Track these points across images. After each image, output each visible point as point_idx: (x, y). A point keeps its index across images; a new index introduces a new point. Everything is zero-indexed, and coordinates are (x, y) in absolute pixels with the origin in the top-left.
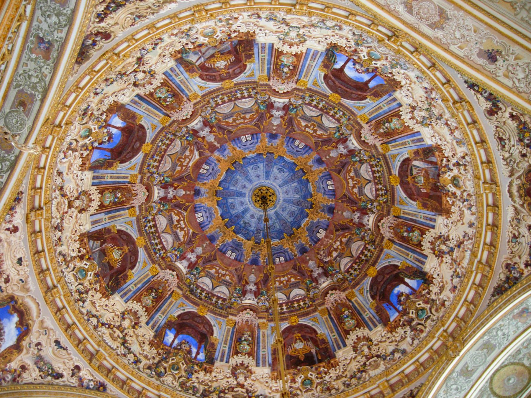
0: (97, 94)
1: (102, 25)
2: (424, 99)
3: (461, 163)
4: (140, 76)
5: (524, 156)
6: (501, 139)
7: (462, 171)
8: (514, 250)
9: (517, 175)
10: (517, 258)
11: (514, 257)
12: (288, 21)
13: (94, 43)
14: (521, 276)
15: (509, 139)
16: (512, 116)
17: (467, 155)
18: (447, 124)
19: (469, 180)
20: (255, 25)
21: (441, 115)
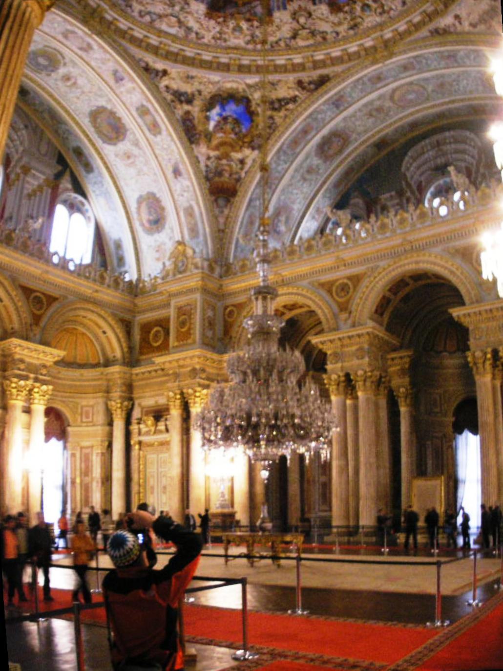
0: (337, 34)
1: (297, 93)
4: (302, 20)
12: (177, 24)
13: (310, 83)
20: (202, 25)
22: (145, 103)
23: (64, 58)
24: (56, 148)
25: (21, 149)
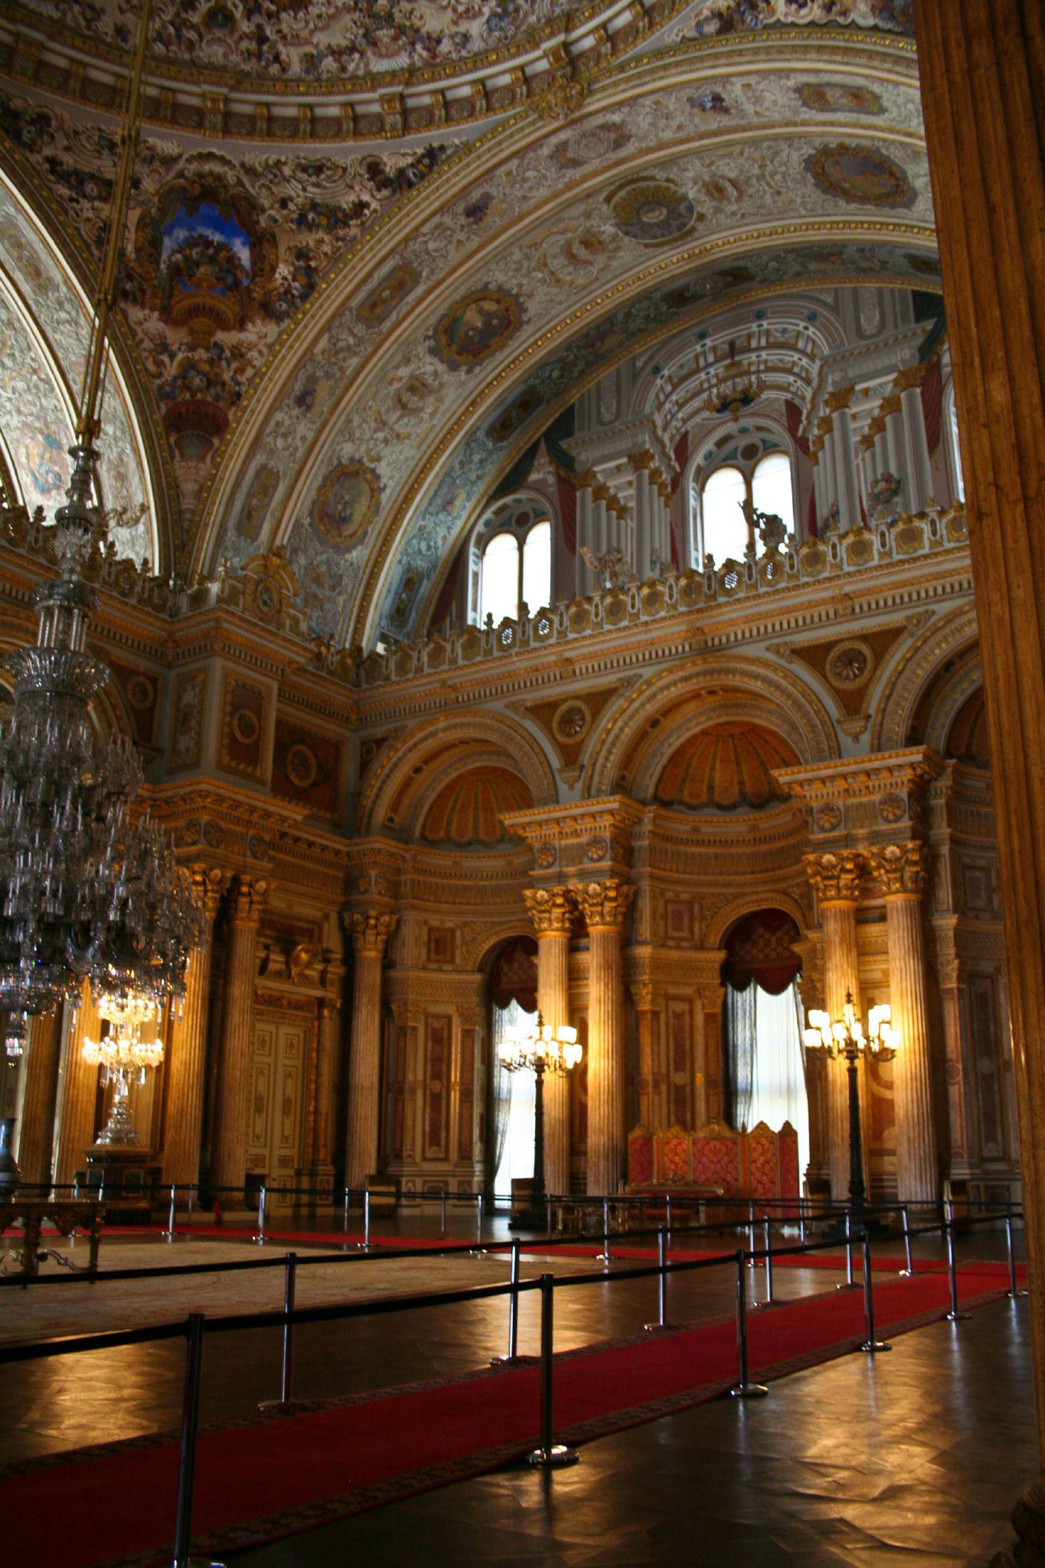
2: (417, 23)
3: (265, 48)
5: (284, 203)
6: (319, 169)
7: (245, 44)
8: (83, 138)
9: (245, 179)
10: (65, 142)
11: (68, 138)
14: (25, 146)
15: (317, 185)
16: (362, 206)
17: (284, 70)
18: (352, 49)
19: (225, 55)
21: (374, 44)
22: (791, 83)
23: (653, 178)
24: (902, 292)
25: (815, 369)
